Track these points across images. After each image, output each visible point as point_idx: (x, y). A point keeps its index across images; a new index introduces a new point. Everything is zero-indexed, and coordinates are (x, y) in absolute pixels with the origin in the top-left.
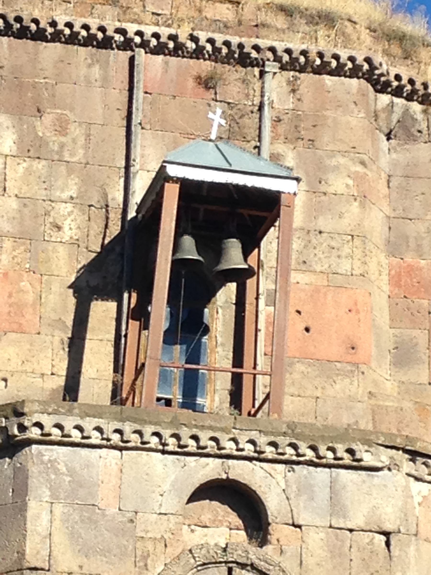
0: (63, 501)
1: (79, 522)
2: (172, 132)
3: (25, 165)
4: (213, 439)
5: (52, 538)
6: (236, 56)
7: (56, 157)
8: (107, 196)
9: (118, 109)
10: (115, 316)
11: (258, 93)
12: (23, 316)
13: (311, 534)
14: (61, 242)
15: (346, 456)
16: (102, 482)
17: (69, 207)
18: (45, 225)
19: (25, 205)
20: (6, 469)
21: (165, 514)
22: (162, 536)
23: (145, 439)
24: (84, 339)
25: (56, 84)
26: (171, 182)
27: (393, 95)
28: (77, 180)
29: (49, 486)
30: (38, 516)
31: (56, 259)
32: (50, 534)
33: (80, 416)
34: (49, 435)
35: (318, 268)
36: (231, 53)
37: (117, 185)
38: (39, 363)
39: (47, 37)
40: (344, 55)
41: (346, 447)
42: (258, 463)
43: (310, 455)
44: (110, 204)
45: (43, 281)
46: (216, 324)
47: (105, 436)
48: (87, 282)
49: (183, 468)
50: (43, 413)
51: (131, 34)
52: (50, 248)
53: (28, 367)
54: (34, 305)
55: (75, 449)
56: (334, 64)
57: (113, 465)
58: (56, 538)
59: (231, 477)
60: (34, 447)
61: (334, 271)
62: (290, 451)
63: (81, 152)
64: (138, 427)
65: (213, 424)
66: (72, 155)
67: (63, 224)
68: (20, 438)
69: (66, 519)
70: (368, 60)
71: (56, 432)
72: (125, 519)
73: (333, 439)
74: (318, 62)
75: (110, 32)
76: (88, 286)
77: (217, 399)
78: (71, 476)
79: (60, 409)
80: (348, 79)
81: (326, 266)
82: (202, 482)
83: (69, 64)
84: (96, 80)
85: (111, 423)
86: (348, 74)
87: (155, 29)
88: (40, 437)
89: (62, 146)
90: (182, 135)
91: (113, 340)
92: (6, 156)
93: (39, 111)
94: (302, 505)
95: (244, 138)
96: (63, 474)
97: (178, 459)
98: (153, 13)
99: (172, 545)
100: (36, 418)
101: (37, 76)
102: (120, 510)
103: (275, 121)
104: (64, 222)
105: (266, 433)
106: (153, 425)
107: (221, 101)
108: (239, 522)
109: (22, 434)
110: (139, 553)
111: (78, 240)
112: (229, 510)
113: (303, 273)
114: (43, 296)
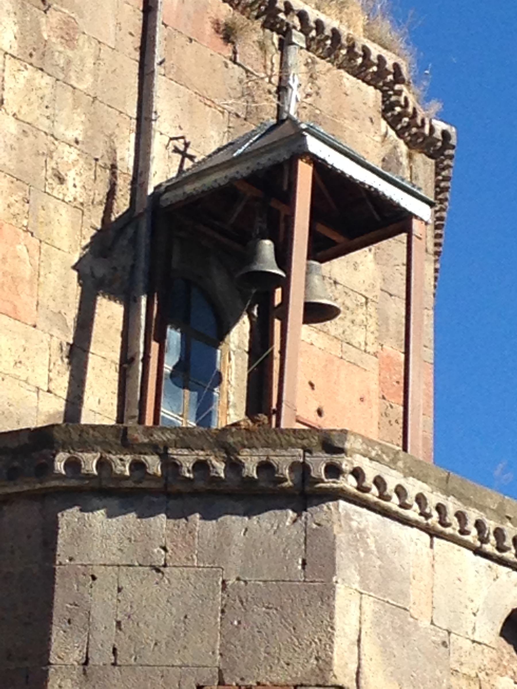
0: (371, 594)
2: (188, 88)
5: (361, 647)
8: (116, 153)
9: (131, 34)
10: (121, 328)
12: (18, 295)
14: (63, 201)
16: (414, 578)
21: (480, 643)
27: (389, 123)
28: (83, 118)
31: (57, 223)
33: (403, 472)
37: (126, 141)
44: (119, 164)
45: (42, 251)
46: (228, 375)
48: (91, 268)
49: (494, 580)
50: (365, 456)
52: (52, 206)
53: (22, 372)
54: (31, 282)
60: (342, 503)
63: (89, 79)
67: (66, 175)
68: (328, 485)
70: (396, 66)
76: (93, 275)
79: (384, 456)
80: (364, 85)
81: (341, 331)
85: (435, 493)
86: (369, 78)
89: (69, 62)
90: (198, 97)
91: (118, 361)
92: (6, 53)
96: (372, 552)
97: (490, 567)
100: (359, 461)
102: (432, 623)
106: (477, 508)
107: (239, 65)
109: (331, 480)
111: (82, 204)
113: (317, 333)
114: (42, 273)
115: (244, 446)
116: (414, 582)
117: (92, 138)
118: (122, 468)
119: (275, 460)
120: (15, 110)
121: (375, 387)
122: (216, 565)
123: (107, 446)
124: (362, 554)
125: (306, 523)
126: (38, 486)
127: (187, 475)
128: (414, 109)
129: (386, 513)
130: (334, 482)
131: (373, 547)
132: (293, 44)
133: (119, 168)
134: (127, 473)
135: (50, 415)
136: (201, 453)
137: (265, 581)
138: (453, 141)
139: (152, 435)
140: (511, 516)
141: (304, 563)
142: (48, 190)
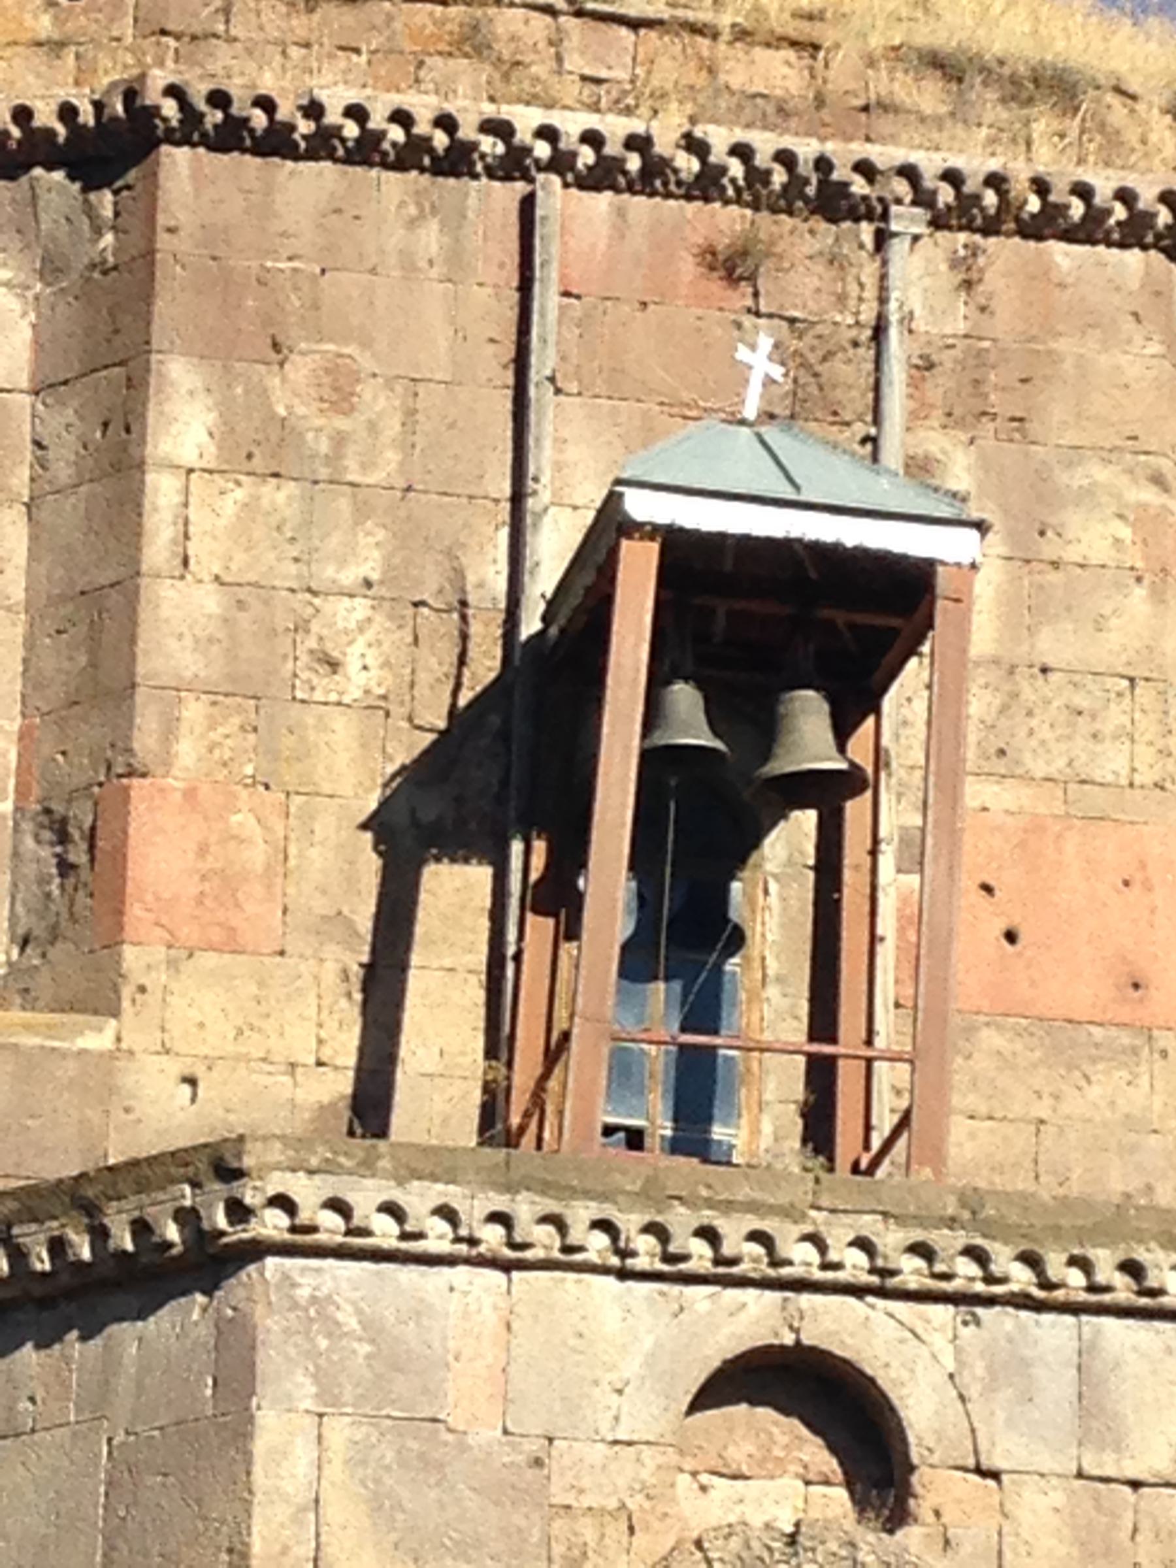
0: (349, 1410)
1: (395, 1467)
2: (639, 401)
3: (239, 494)
4: (756, 1236)
5: (321, 1511)
6: (811, 191)
7: (324, 473)
8: (464, 578)
9: (492, 340)
10: (488, 903)
11: (870, 293)
12: (237, 905)
13: (1026, 1494)
14: (339, 704)
15: (1120, 1280)
16: (457, 1359)
17: (361, 607)
18: (296, 659)
19: (241, 604)
20: (196, 1324)
21: (630, 1444)
22: (623, 1506)
23: (574, 1238)
24: (404, 967)
25: (323, 271)
26: (637, 535)
28: (381, 535)
29: (311, 1368)
30: (281, 1454)
31: (326, 751)
32: (317, 1501)
33: (395, 1179)
34: (313, 1229)
35: (1039, 769)
36: (796, 182)
37: (489, 547)
38: (282, 1034)
39: (296, 145)
40: (1104, 186)
41: (1121, 1256)
42: (881, 1303)
43: (1021, 1278)
44: (471, 599)
45: (293, 810)
46: (763, 924)
47: (463, 1232)
48: (413, 811)
51: (523, 135)
52: (311, 721)
53: (254, 1046)
55: (384, 1266)
56: (1077, 209)
57: (487, 1311)
58: (332, 1512)
59: (806, 1341)
60: (271, 1262)
61: (1083, 777)
62: (967, 1268)
63: (392, 457)
64: (552, 1206)
65: (757, 1195)
66: (366, 467)
67: (345, 654)
68: (235, 1238)
69: (358, 1459)
71: (331, 1220)
72: (520, 1459)
73: (1083, 1235)
74: (1034, 204)
75: (467, 131)
76: (415, 823)
77: (767, 1127)
78: (372, 1341)
79: (342, 1160)
80: (1115, 251)
81: (1061, 763)
82: (729, 1356)
83: (357, 218)
84: (431, 263)
86: (1116, 236)
87: (591, 121)
88: (287, 1236)
89: (340, 440)
90: (665, 409)
91: (484, 968)
92: (190, 471)
93: (276, 346)
94: (1001, 1415)
95: (835, 413)
98: (584, 78)
99: (647, 1528)
100: (276, 1184)
101: (273, 254)
102: (506, 1432)
103: (917, 367)
104: (349, 650)
105: (901, 1220)
106: (592, 1199)
107: (770, 316)
108: (830, 1464)
109: (239, 1228)
110: (558, 1549)
111: (384, 697)
112: (804, 1432)
113: (998, 783)
114: (293, 850)
115: (110, 1199)
127: (38, 1266)
130: (244, 1230)
131: (353, 1323)
132: (895, 235)
135: (322, 1107)
136: (55, 1224)
137: (161, 1428)
140: (683, 1194)
142: (299, 695)
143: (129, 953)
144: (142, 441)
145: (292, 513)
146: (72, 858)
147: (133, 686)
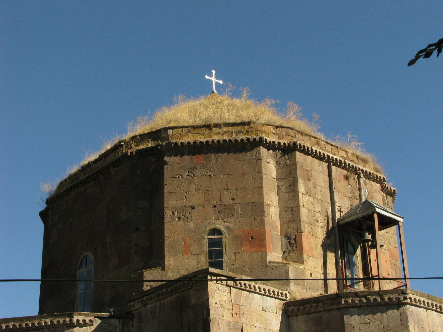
9: (327, 183)
52: (317, 228)
53: (316, 270)
60: (407, 305)
63: (320, 195)
68: (404, 302)
70: (384, 178)
76: (327, 243)
89: (315, 193)
93: (308, 179)
102: (429, 330)
107: (350, 185)
111: (323, 227)
115: (384, 294)
116: (424, 321)
117: (323, 210)
118: (357, 301)
119: (392, 297)
120: (306, 207)
121: (388, 258)
122: (381, 322)
123: (353, 297)
124: (413, 316)
125: (400, 311)
126: (338, 307)
127: (372, 302)
128: (387, 186)
129: (417, 306)
133: (329, 216)
134: (358, 302)
136: (375, 297)
138: (396, 192)
139: (363, 293)
141: (401, 320)
143: (304, 256)
144: (298, 188)
145: (312, 201)
146: (292, 242)
147: (300, 221)
